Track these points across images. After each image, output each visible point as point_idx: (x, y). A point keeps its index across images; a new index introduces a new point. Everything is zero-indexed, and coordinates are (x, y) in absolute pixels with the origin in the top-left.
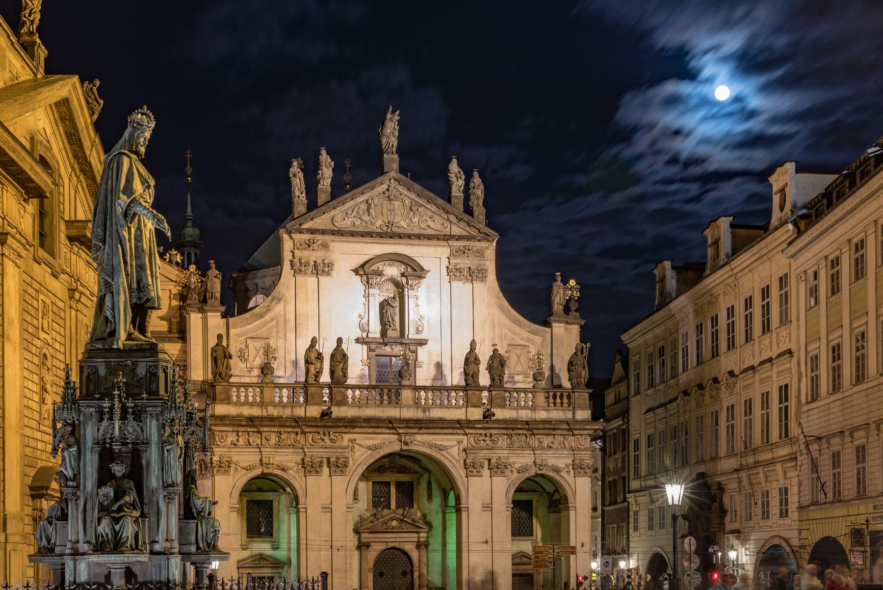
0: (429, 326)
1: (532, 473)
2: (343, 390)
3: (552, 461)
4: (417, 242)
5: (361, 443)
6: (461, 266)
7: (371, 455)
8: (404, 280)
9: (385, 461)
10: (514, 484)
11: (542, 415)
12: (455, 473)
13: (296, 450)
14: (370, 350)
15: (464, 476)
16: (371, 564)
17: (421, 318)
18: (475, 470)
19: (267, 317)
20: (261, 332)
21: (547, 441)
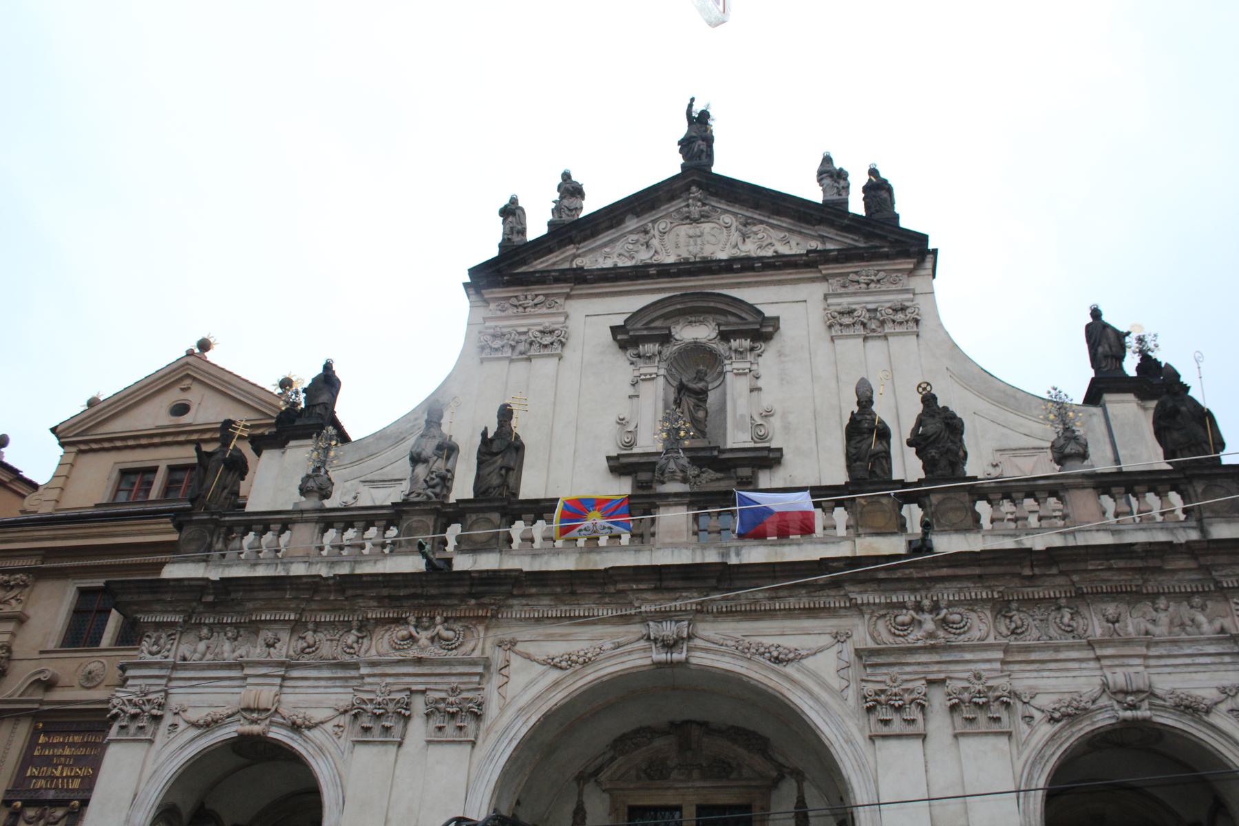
0: (787, 428)
1: (1103, 720)
2: (495, 517)
4: (749, 277)
5: (531, 649)
6: (854, 307)
7: (556, 684)
8: (721, 348)
9: (659, 743)
10: (1040, 756)
12: (829, 731)
13: (340, 673)
15: (861, 740)
17: (768, 414)
18: (896, 718)
21: (1133, 624)
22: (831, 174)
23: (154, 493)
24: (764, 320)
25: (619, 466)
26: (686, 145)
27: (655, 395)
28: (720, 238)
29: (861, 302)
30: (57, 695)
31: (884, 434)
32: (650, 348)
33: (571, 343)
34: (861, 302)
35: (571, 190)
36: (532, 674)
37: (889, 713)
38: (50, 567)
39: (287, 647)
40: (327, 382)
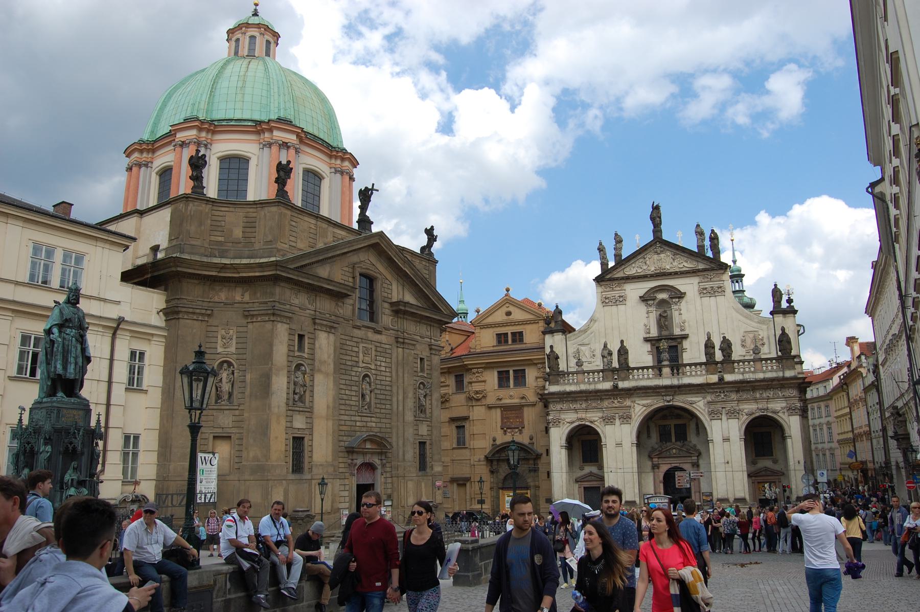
1: (757, 415)
3: (771, 406)
11: (760, 376)
14: (652, 345)
16: (661, 478)
19: (589, 332)
20: (586, 341)
22: (700, 233)
23: (510, 342)
24: (682, 293)
25: (646, 340)
26: (652, 219)
27: (653, 317)
28: (667, 261)
29: (708, 285)
30: (503, 402)
31: (714, 348)
32: (651, 302)
33: (628, 299)
34: (708, 285)
35: (618, 240)
36: (640, 409)
37: (714, 415)
38: (489, 366)
39: (584, 406)
40: (558, 312)
